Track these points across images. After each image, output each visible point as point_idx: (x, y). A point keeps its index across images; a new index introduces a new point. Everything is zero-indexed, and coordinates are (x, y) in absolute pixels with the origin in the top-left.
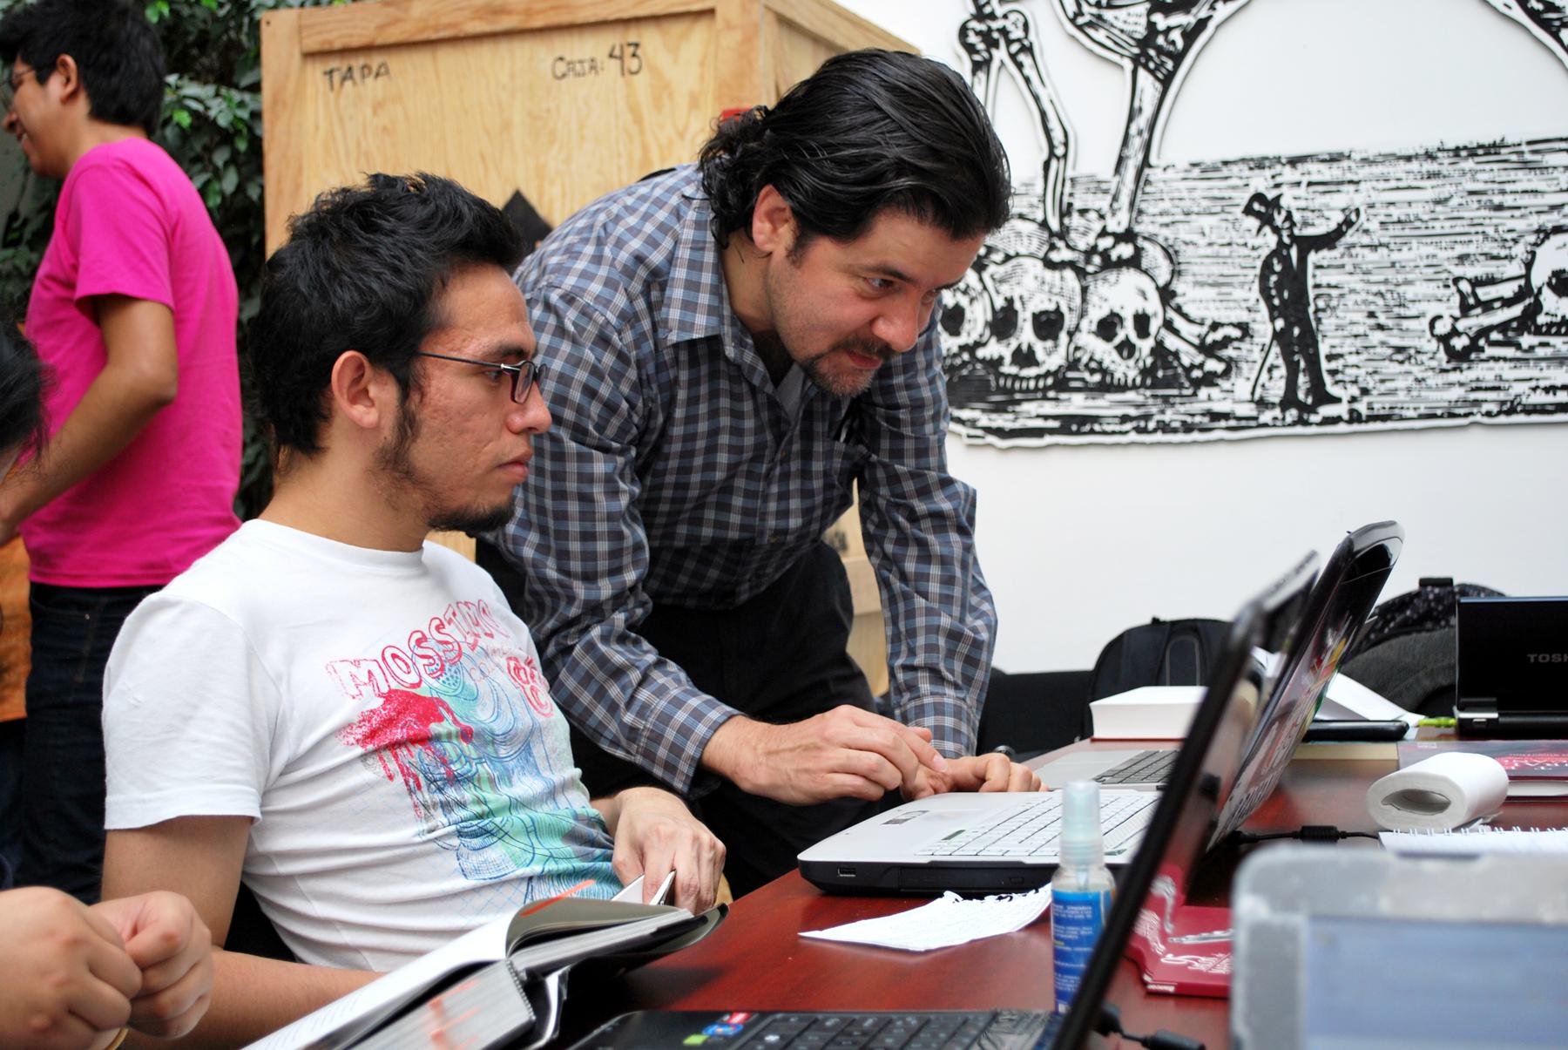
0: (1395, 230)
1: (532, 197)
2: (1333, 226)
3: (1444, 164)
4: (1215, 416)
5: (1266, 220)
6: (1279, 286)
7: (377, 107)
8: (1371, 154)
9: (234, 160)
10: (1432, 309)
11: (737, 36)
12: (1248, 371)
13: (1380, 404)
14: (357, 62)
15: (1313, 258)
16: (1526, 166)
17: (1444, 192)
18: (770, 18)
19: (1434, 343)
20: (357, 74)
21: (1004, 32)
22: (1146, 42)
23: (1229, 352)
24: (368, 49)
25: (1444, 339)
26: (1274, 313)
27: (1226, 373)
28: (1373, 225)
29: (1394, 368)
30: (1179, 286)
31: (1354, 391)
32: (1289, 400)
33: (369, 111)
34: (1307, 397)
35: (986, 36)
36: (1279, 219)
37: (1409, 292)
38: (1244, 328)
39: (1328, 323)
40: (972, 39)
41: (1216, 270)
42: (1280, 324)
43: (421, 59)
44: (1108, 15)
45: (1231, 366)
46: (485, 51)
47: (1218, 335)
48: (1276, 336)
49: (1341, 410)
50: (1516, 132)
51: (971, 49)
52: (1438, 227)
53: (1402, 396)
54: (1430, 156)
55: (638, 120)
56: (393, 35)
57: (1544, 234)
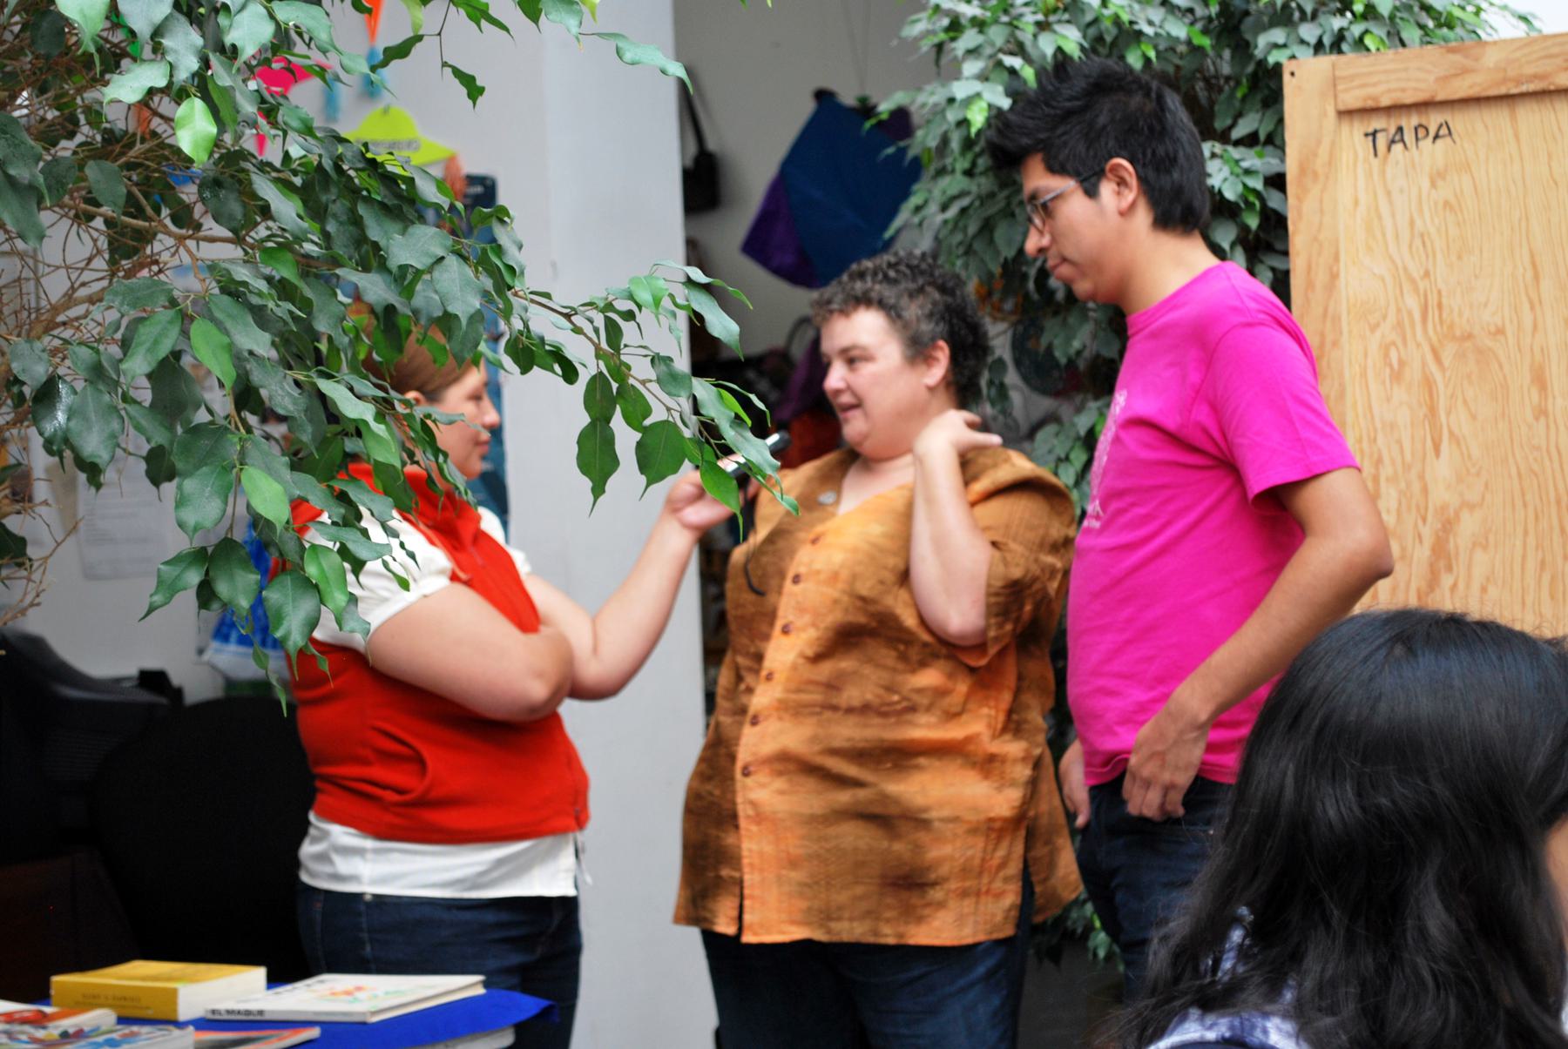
7: (1436, 178)
14: (1410, 122)
20: (1409, 136)
33: (1426, 183)
43: (1498, 117)
56: (1461, 88)
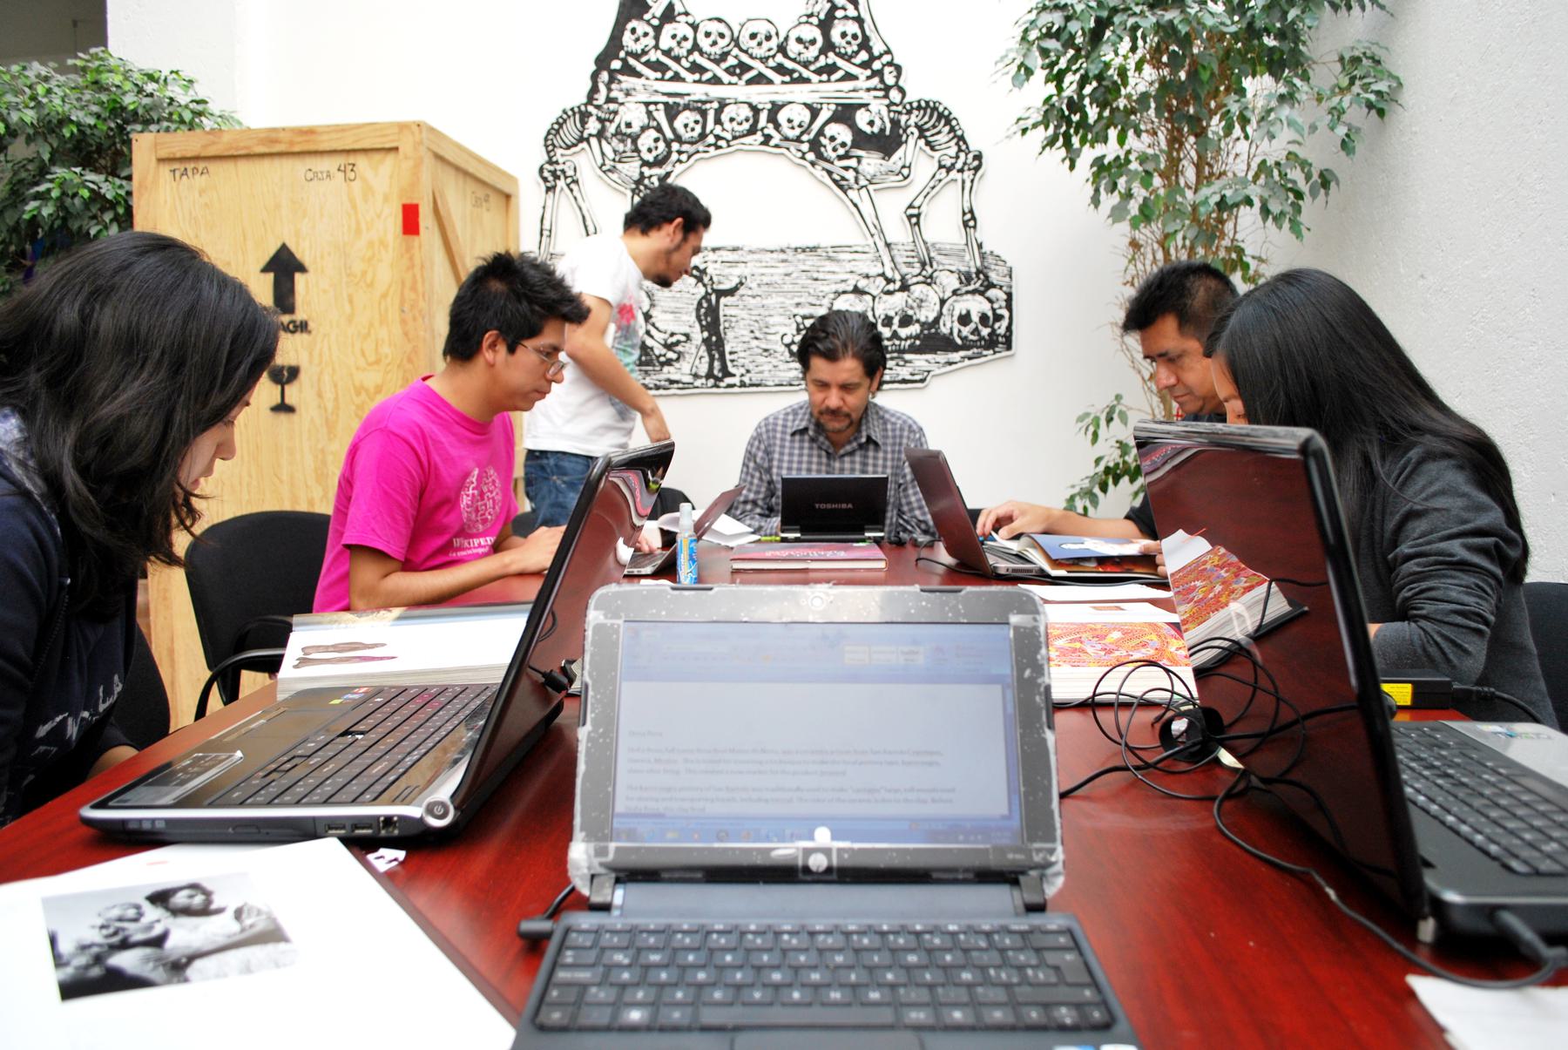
0: (765, 288)
1: (293, 248)
2: (733, 285)
3: (789, 255)
4: (672, 382)
5: (700, 280)
6: (706, 315)
8: (753, 248)
9: (116, 219)
10: (783, 330)
11: (411, 163)
12: (689, 358)
13: (756, 378)
14: (190, 166)
15: (723, 300)
16: (830, 258)
17: (790, 270)
18: (430, 155)
19: (783, 348)
21: (563, 171)
22: (639, 182)
23: (679, 348)
24: (197, 158)
25: (788, 346)
26: (703, 329)
27: (678, 360)
28: (754, 285)
29: (763, 359)
30: (653, 312)
31: (743, 371)
32: (710, 375)
34: (719, 373)
35: (554, 173)
36: (706, 280)
37: (771, 321)
38: (687, 335)
39: (730, 335)
40: (546, 174)
41: (673, 305)
42: (706, 334)
43: (228, 166)
44: (619, 166)
45: (680, 354)
46: (266, 163)
47: (674, 339)
48: (705, 341)
49: (736, 380)
50: (825, 241)
51: (545, 180)
52: (786, 288)
53: (766, 374)
54: (783, 251)
55: (354, 207)
56: (212, 151)
57: (838, 294)
